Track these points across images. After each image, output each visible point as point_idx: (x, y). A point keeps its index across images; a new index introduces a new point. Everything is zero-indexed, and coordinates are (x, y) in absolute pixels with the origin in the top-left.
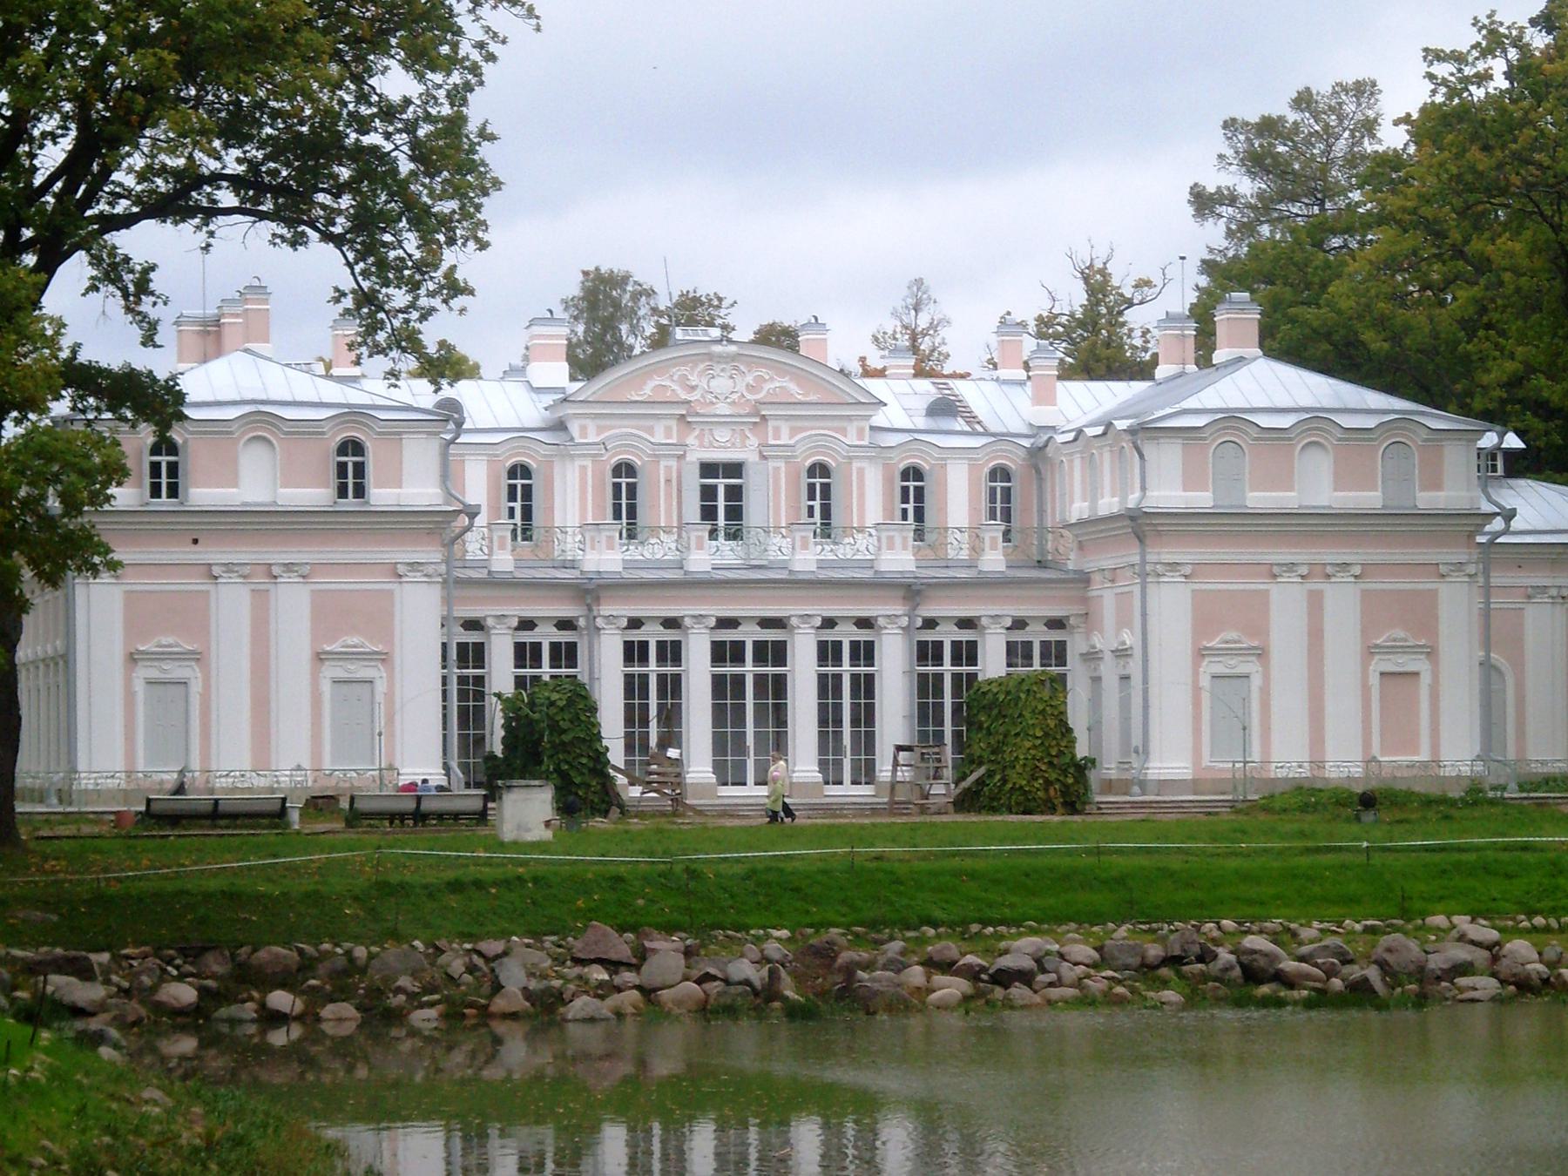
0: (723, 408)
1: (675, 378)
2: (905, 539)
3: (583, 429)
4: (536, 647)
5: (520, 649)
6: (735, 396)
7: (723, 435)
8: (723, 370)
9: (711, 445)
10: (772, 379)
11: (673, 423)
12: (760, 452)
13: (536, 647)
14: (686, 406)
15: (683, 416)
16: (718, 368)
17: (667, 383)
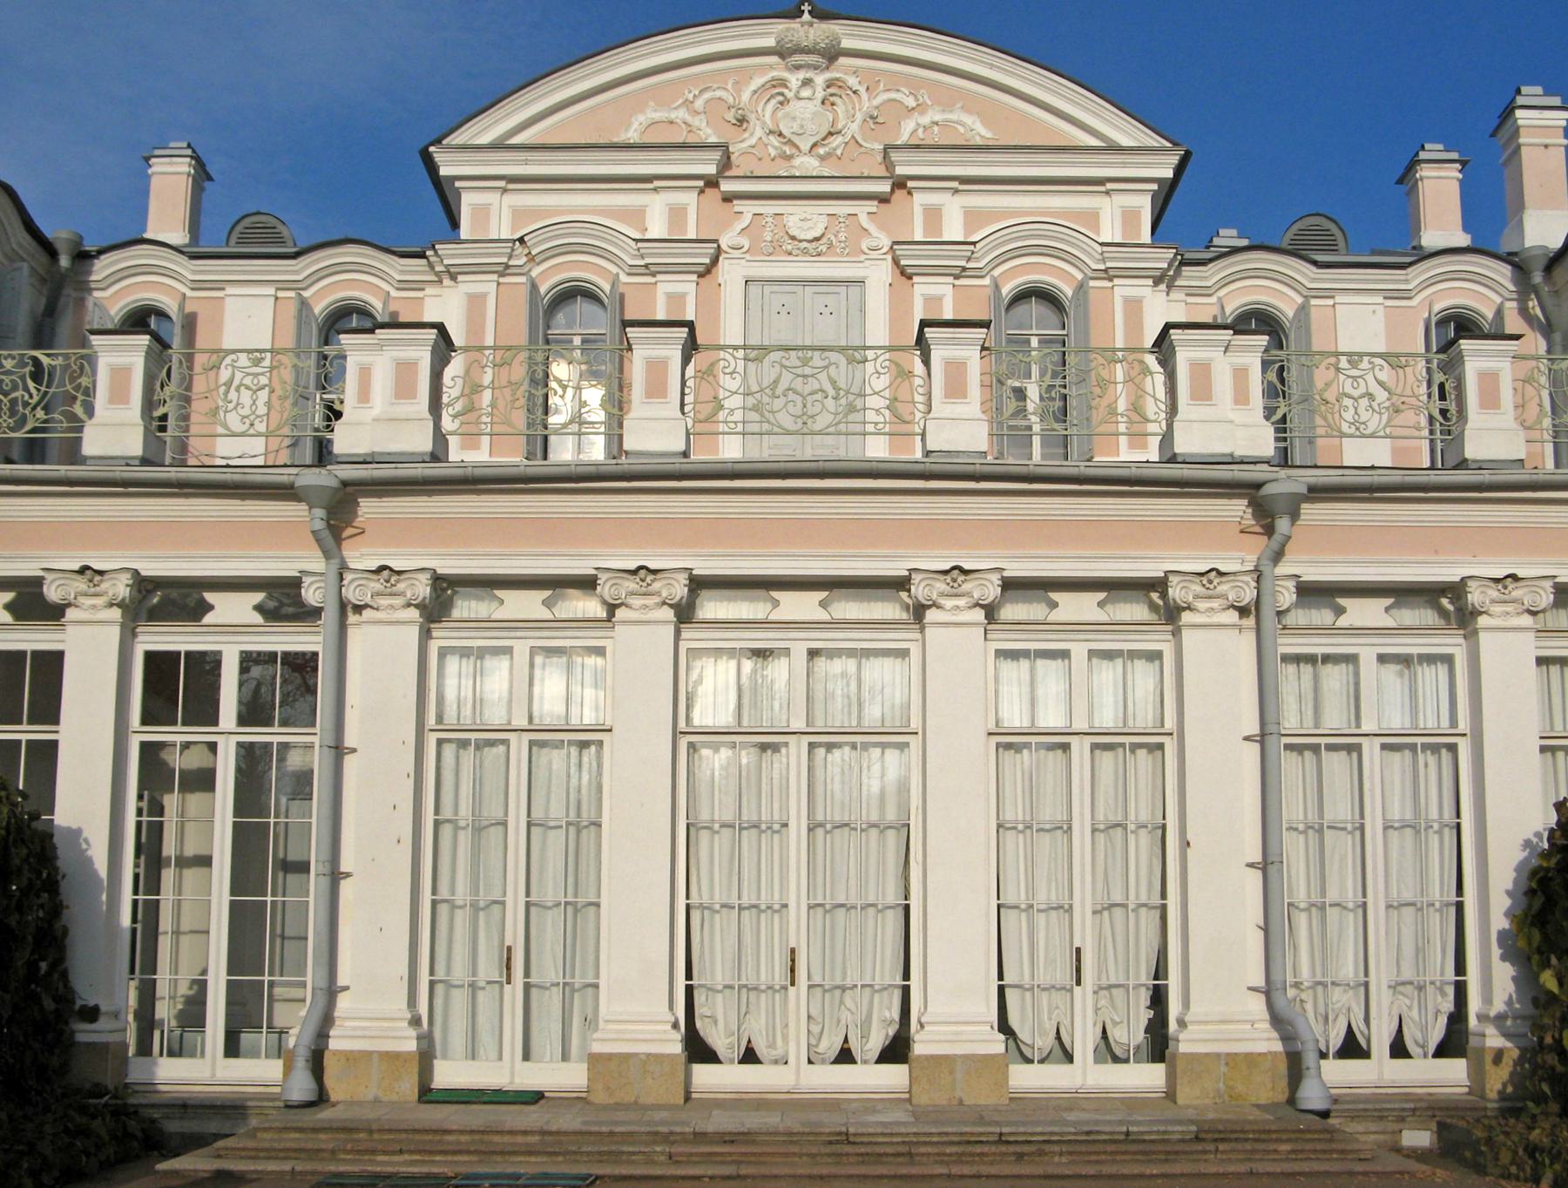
0: (808, 164)
1: (699, 104)
2: (1240, 374)
3: (482, 212)
4: (205, 667)
5: (160, 667)
6: (836, 141)
7: (805, 220)
8: (807, 82)
9: (775, 248)
10: (920, 108)
11: (689, 199)
12: (896, 262)
13: (205, 667)
14: (717, 155)
15: (711, 183)
16: (794, 79)
17: (681, 114)
